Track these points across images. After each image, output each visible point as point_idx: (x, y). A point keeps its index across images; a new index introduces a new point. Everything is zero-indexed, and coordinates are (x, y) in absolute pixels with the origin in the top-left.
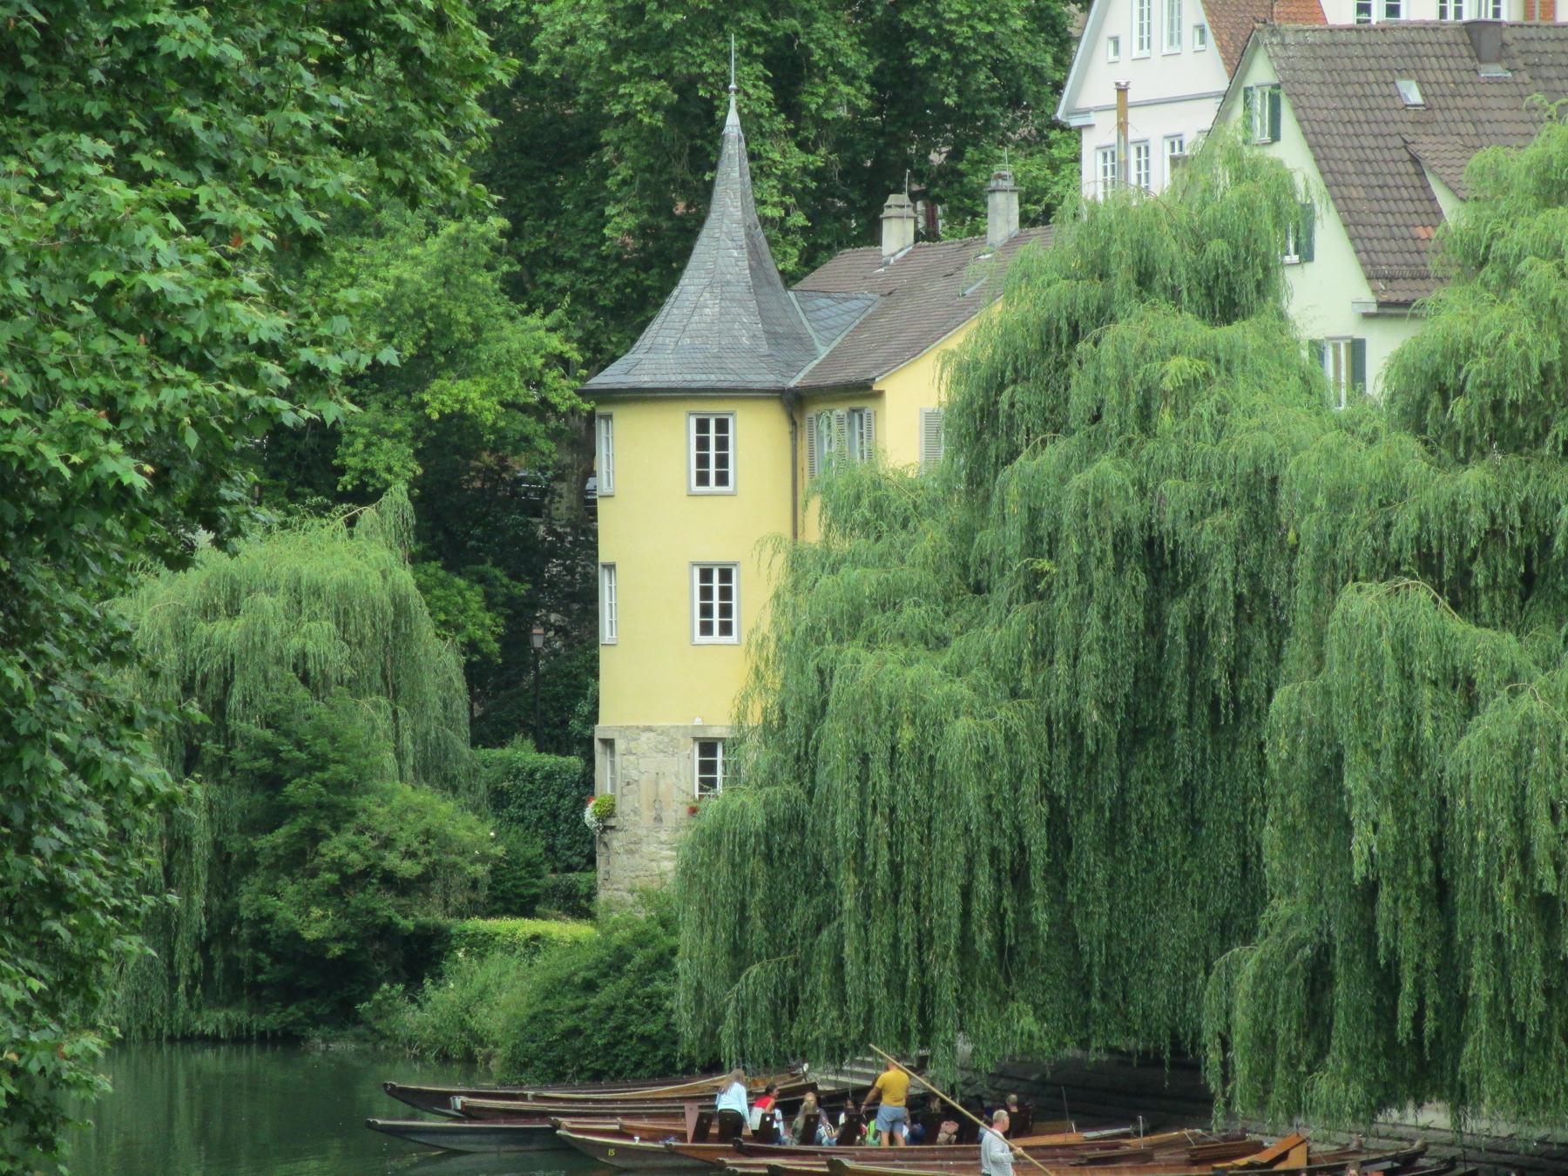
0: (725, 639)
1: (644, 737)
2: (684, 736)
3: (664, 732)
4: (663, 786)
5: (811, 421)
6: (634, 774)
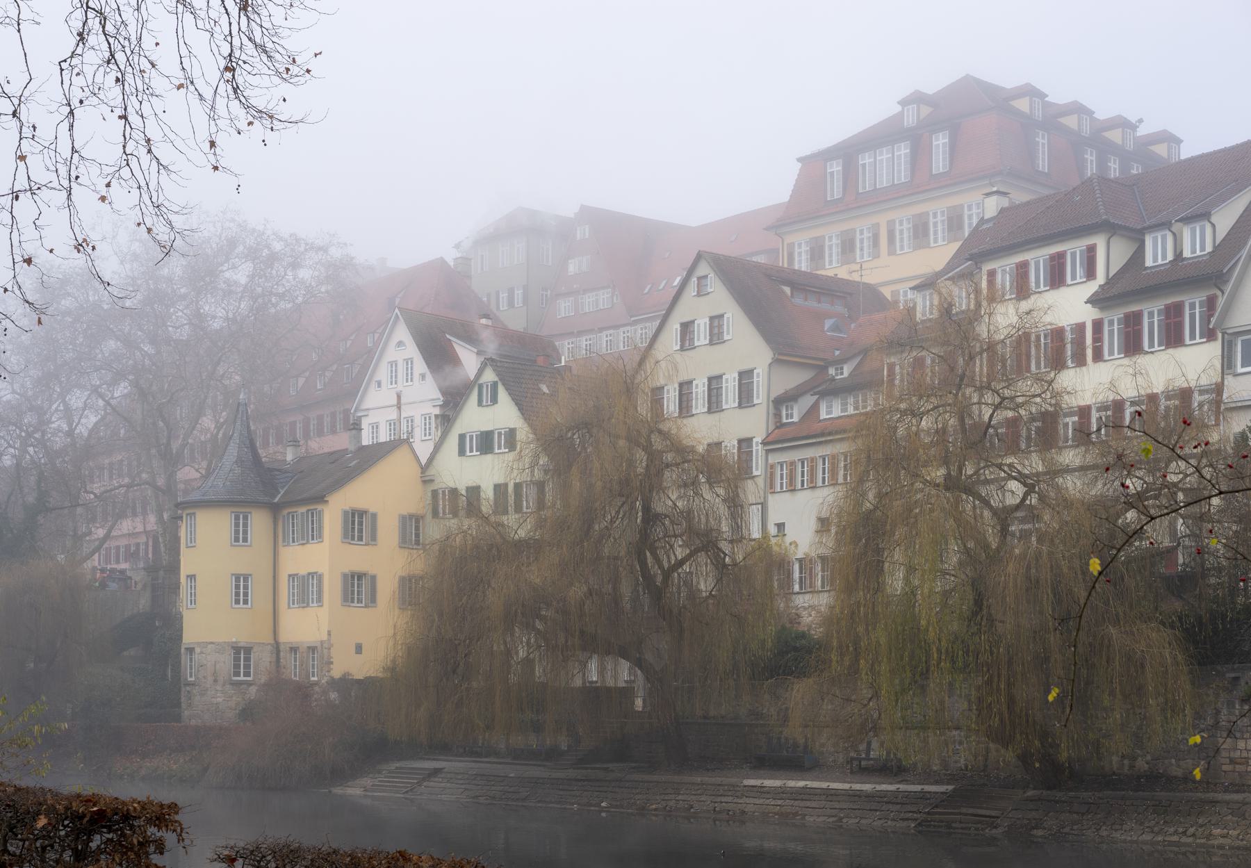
3: (219, 644)
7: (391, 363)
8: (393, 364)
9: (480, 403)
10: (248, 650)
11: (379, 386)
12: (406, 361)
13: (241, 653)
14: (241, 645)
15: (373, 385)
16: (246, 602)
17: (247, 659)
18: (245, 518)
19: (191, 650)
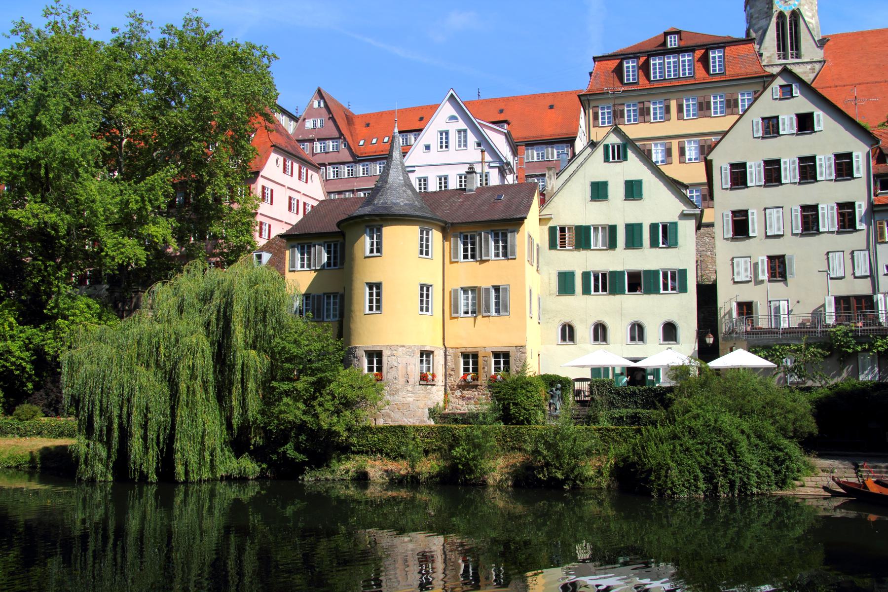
1: (400, 349)
3: (410, 347)
9: (606, 159)
11: (428, 147)
12: (459, 131)
14: (428, 348)
16: (427, 310)
18: (427, 234)
19: (375, 356)
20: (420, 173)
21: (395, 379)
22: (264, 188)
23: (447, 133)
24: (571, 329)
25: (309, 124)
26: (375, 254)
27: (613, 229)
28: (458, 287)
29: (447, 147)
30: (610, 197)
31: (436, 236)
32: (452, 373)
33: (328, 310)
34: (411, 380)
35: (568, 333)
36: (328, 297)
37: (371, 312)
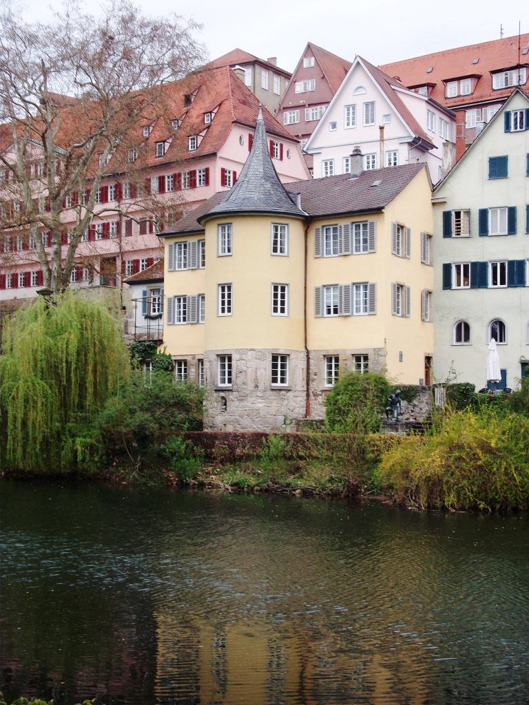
0: (282, 314)
1: (250, 353)
2: (269, 353)
4: (259, 373)
5: (317, 230)
6: (244, 368)
7: (348, 107)
8: (351, 108)
10: (284, 358)
11: (334, 125)
12: (367, 104)
13: (279, 361)
14: (282, 352)
15: (328, 127)
16: (283, 311)
17: (283, 366)
20: (326, 155)
21: (244, 384)
22: (223, 171)
23: (354, 107)
24: (467, 327)
25: (299, 88)
26: (227, 253)
27: (512, 212)
28: (319, 285)
29: (353, 124)
30: (509, 175)
31: (294, 231)
32: (315, 377)
33: (358, 303)
34: (261, 386)
35: (463, 332)
36: (358, 288)
37: (223, 314)
